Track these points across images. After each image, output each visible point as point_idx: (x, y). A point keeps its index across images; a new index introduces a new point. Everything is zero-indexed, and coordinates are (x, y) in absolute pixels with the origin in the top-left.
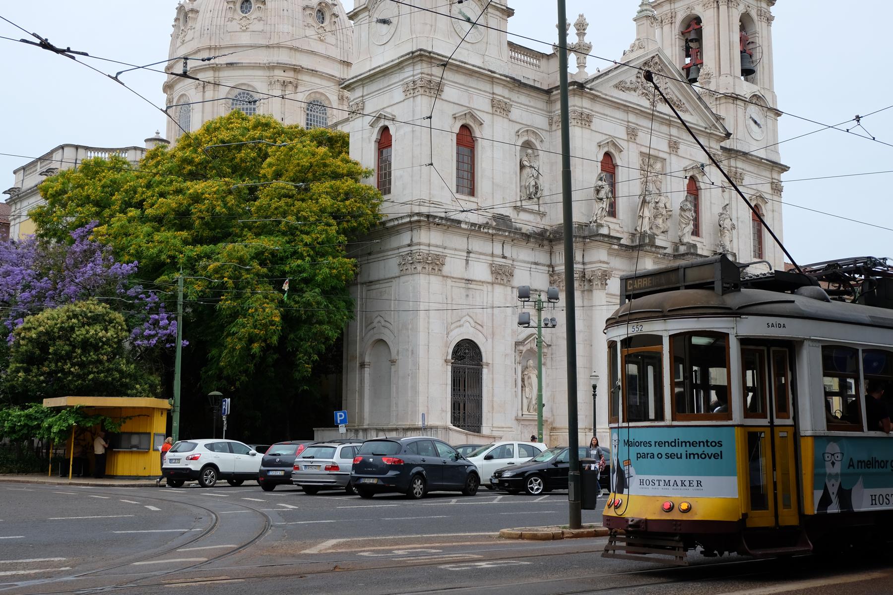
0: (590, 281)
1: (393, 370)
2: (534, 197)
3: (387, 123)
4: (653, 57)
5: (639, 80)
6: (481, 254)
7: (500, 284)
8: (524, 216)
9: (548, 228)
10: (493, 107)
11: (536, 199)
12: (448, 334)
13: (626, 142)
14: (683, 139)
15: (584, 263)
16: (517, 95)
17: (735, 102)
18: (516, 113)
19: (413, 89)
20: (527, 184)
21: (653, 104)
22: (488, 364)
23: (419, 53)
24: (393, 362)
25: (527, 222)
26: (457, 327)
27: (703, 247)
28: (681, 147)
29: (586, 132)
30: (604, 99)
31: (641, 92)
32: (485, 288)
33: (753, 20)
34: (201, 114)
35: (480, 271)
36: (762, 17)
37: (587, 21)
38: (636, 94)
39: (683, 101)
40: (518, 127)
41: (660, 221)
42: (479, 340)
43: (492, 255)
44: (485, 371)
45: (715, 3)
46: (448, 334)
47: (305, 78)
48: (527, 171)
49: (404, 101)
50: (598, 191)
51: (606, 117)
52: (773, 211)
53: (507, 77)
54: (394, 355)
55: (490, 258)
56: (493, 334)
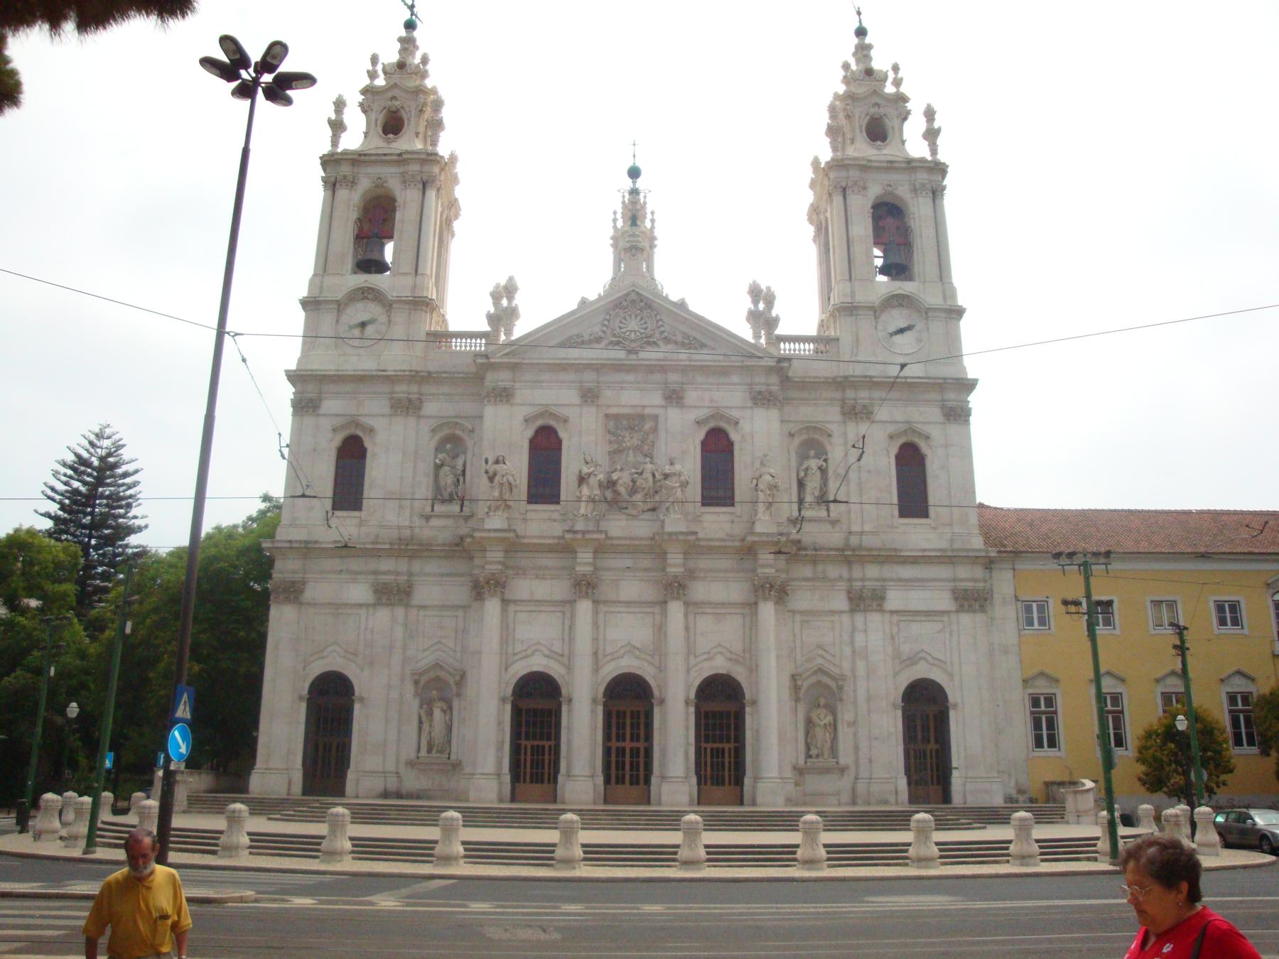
2: (456, 497)
4: (627, 294)
5: (605, 329)
6: (356, 573)
7: (387, 605)
12: (304, 668)
14: (693, 384)
18: (431, 408)
21: (630, 352)
22: (362, 699)
26: (318, 659)
29: (503, 410)
32: (363, 612)
35: (360, 592)
38: (603, 345)
41: (638, 497)
42: (350, 671)
46: (304, 668)
52: (946, 446)
53: (404, 371)
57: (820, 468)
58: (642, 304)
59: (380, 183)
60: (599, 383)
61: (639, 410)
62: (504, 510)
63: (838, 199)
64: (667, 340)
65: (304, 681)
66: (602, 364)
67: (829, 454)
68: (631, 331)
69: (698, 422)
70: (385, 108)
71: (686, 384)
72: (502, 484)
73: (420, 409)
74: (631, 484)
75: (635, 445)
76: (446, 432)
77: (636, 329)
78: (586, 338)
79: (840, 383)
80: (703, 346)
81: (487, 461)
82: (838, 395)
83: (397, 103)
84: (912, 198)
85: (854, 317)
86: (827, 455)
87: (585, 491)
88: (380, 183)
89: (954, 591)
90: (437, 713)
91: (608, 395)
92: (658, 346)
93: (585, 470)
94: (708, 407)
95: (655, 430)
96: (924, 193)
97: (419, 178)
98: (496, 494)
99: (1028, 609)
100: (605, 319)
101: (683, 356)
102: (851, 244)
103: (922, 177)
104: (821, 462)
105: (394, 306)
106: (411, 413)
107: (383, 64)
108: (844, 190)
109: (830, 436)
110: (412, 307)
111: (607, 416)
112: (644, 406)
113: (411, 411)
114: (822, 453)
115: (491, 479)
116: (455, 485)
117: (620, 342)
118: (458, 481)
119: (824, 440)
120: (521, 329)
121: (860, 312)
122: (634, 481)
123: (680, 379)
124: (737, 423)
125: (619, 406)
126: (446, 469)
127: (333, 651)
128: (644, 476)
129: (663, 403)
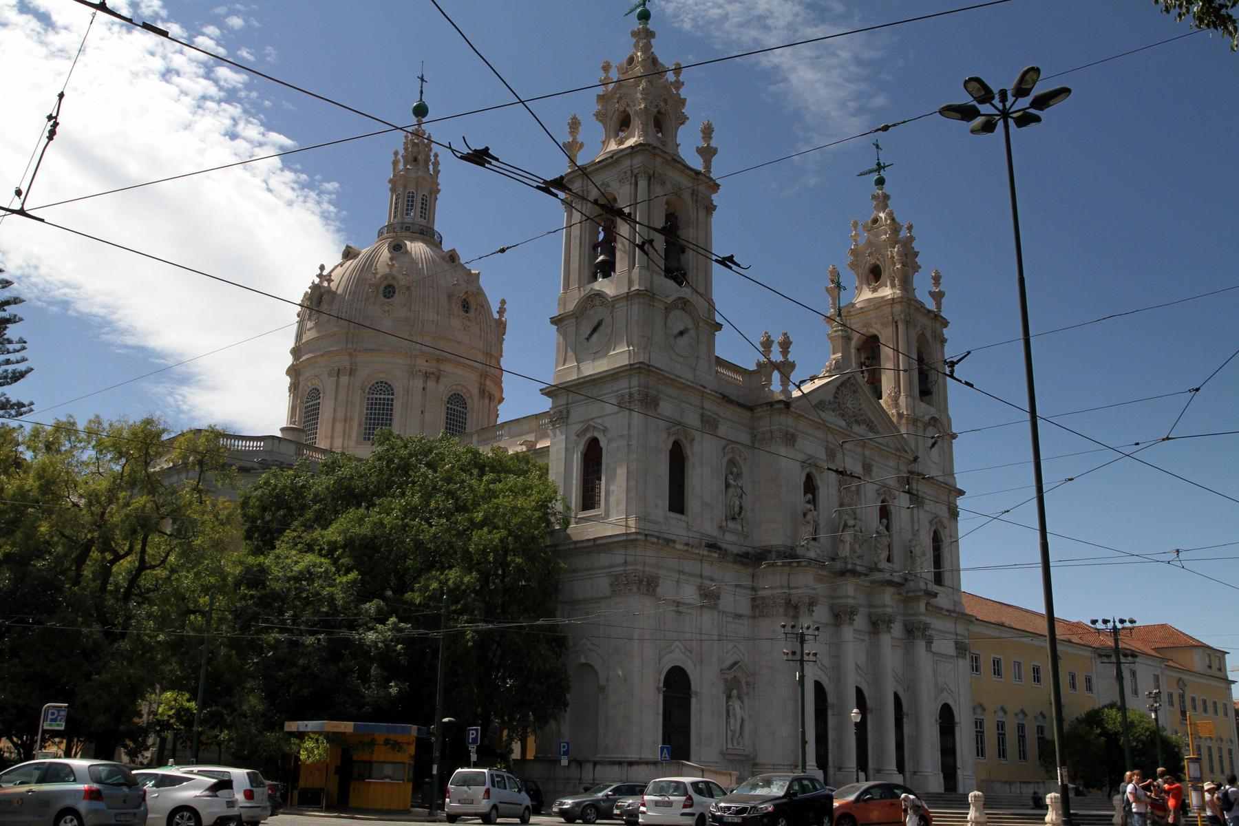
0: (796, 607)
1: (601, 697)
3: (596, 434)
4: (849, 378)
8: (729, 537)
9: (750, 550)
10: (702, 422)
11: (739, 520)
12: (660, 660)
15: (789, 588)
18: (722, 430)
19: (629, 402)
20: (732, 503)
21: (848, 424)
22: (696, 693)
23: (638, 366)
24: (602, 689)
25: (730, 542)
28: (875, 469)
30: (806, 418)
31: (838, 413)
34: (333, 402)
35: (689, 593)
37: (791, 339)
39: (876, 423)
40: (723, 442)
42: (689, 667)
43: (701, 576)
44: (693, 700)
46: (660, 660)
47: (447, 367)
48: (731, 491)
49: (618, 413)
50: (805, 515)
53: (716, 392)
54: (602, 682)
55: (699, 580)
56: (701, 661)
65: (660, 675)
80: (877, 433)
89: (956, 643)
90: (737, 707)
99: (972, 657)
100: (836, 393)
101: (871, 436)
127: (677, 646)
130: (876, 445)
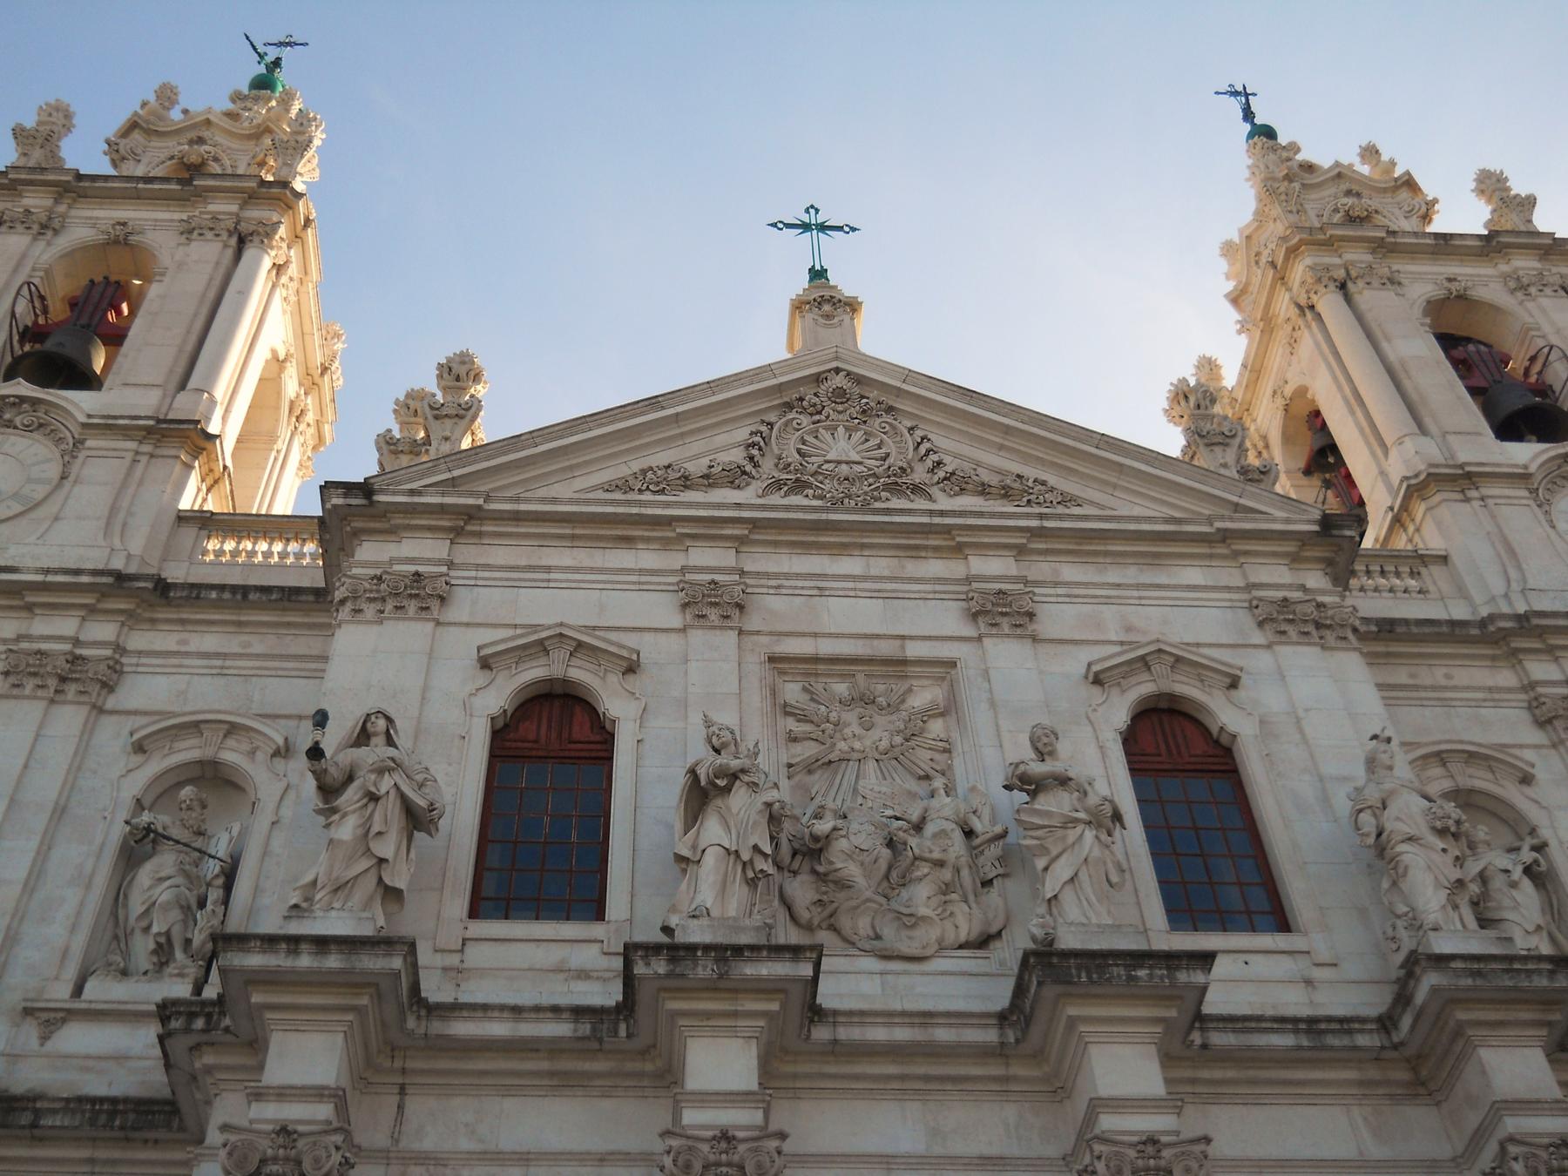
4: (818, 379)
5: (755, 452)
8: (77, 1038)
13: (673, 636)
14: (1056, 584)
16: (175, 637)
17: (1473, 493)
27: (1319, 974)
30: (517, 517)
33: (1495, 309)
36: (1533, 290)
39: (1031, 472)
41: (921, 896)
45: (1307, 310)
51: (545, 576)
53: (77, 572)
57: (1528, 871)
58: (865, 401)
59: (121, 241)
60: (742, 573)
61: (886, 649)
62: (367, 905)
63: (1329, 304)
64: (957, 483)
66: (755, 524)
67: (1545, 833)
68: (839, 462)
69: (1097, 681)
70: (172, 158)
71: (1037, 583)
72: (373, 798)
73: (108, 687)
74: (886, 853)
75: (884, 744)
76: (188, 751)
77: (857, 458)
78: (696, 468)
79: (1501, 638)
81: (321, 719)
82: (1505, 677)
83: (207, 148)
84: (1521, 303)
85: (1476, 504)
86: (1533, 831)
87: (712, 830)
88: (121, 241)
91: (772, 609)
92: (930, 498)
93: (708, 763)
94: (1122, 643)
95: (948, 709)
96: (1548, 291)
97: (230, 224)
98: (346, 830)
102: (1402, 376)
103: (1525, 264)
104: (1527, 856)
105: (89, 443)
106: (71, 695)
107: (185, 112)
108: (1343, 287)
109: (1526, 779)
110: (146, 448)
111: (772, 659)
112: (903, 638)
113: (71, 689)
114: (1516, 826)
115: (329, 791)
116: (186, 909)
117: (809, 486)
118: (202, 904)
119: (1512, 793)
120: (486, 430)
121: (1485, 491)
122: (890, 843)
123: (1014, 571)
124: (1234, 684)
125: (815, 635)
126: (165, 862)
128: (930, 829)
129: (969, 631)
130: (1034, 523)
